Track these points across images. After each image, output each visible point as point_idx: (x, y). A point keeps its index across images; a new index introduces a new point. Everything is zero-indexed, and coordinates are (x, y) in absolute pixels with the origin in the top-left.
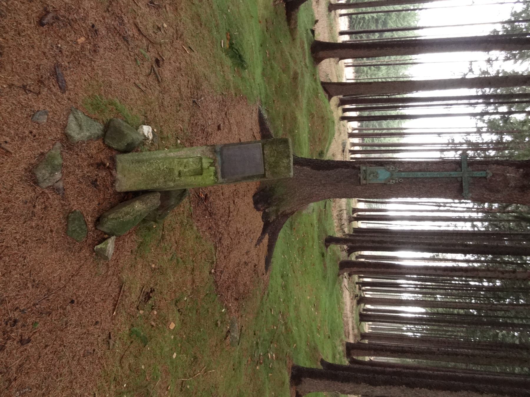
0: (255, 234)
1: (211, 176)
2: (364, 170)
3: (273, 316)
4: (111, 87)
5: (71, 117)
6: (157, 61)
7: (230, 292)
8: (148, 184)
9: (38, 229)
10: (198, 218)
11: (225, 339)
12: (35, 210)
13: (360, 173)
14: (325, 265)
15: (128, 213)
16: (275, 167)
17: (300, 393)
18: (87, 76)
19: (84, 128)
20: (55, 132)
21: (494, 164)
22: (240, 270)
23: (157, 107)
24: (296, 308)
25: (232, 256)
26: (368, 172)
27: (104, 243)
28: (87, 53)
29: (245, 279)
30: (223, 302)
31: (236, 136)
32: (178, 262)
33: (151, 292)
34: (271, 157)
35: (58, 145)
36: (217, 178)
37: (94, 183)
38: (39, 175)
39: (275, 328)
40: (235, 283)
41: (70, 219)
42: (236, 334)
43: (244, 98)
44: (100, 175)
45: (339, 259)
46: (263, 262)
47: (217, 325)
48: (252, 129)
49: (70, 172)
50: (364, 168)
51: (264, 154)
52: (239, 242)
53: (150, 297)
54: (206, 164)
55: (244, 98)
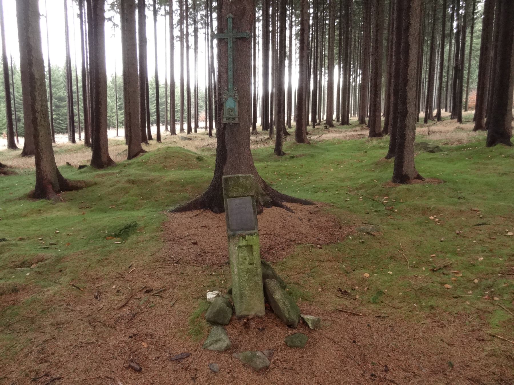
0: (284, 213)
1: (253, 239)
2: (227, 119)
3: (351, 199)
4: (179, 324)
5: (211, 348)
6: (147, 292)
7: (334, 233)
9: (302, 365)
10: (276, 258)
11: (374, 236)
12: (288, 367)
14: (301, 156)
15: (284, 303)
16: (246, 188)
17: (415, 176)
18: (173, 340)
20: (225, 357)
21: (221, 12)
22: (316, 225)
24: (342, 180)
25: (304, 232)
26: (228, 116)
28: (154, 340)
29: (322, 221)
30: (344, 238)
33: (341, 291)
35: (235, 355)
36: (255, 233)
37: (261, 330)
38: (261, 366)
40: (326, 229)
41: (292, 344)
42: (370, 228)
43: (163, 224)
44: (254, 326)
45: (294, 143)
46: (306, 207)
47: (363, 242)
48: (191, 218)
49: (256, 346)
50: (225, 120)
51: (236, 197)
52: (292, 226)
53: (345, 292)
54: (243, 243)
55: (163, 224)
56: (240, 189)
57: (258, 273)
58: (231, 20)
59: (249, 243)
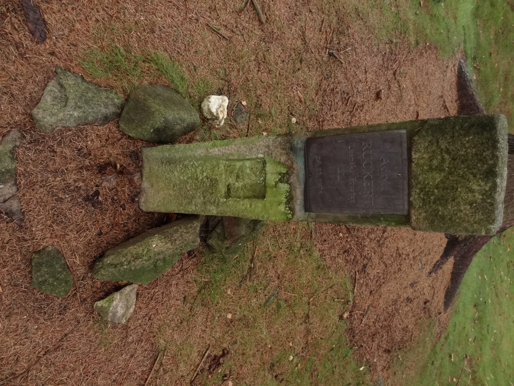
0: (430, 257)
1: (280, 203)
3: (454, 364)
4: (153, 32)
5: (52, 86)
7: (377, 341)
8: (181, 204)
10: (324, 237)
15: (137, 257)
16: (442, 201)
18: (102, 12)
19: (71, 103)
22: (397, 310)
23: (252, 65)
24: (495, 346)
25: (384, 289)
27: (107, 299)
29: (406, 321)
30: (362, 356)
31: (411, 108)
32: (279, 306)
33: (223, 355)
34: (431, 169)
36: (292, 209)
37: (92, 199)
39: (455, 380)
40: (388, 328)
43: (433, 48)
46: (441, 295)
48: (442, 97)
51: (410, 160)
52: (400, 270)
53: (219, 364)
54: (272, 178)
55: (433, 48)
56: (438, 177)
57: (208, 207)
59: (269, 192)
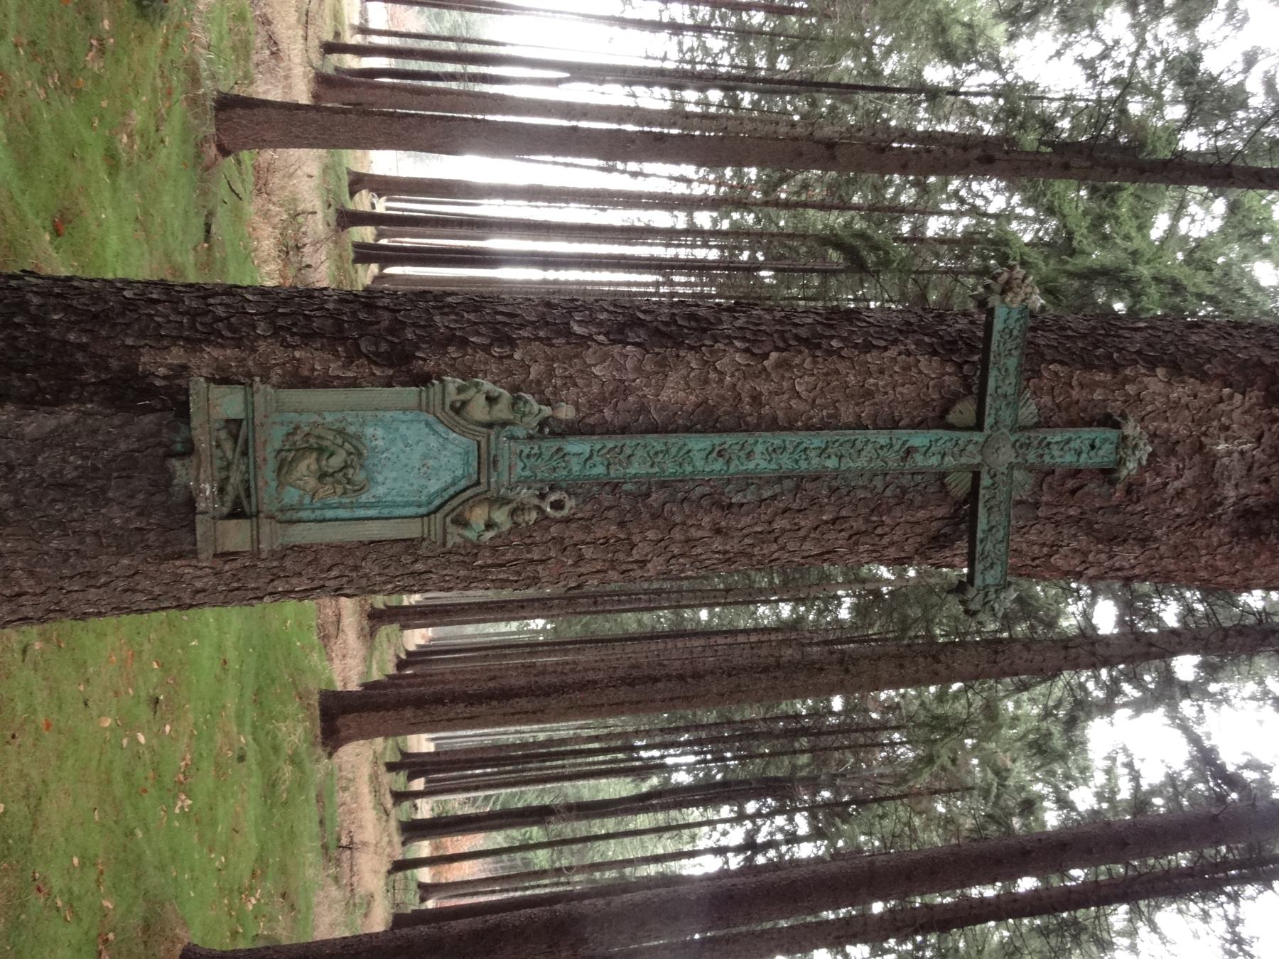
2: (233, 426)
13: (189, 450)
26: (273, 438)
58: (1105, 455)
